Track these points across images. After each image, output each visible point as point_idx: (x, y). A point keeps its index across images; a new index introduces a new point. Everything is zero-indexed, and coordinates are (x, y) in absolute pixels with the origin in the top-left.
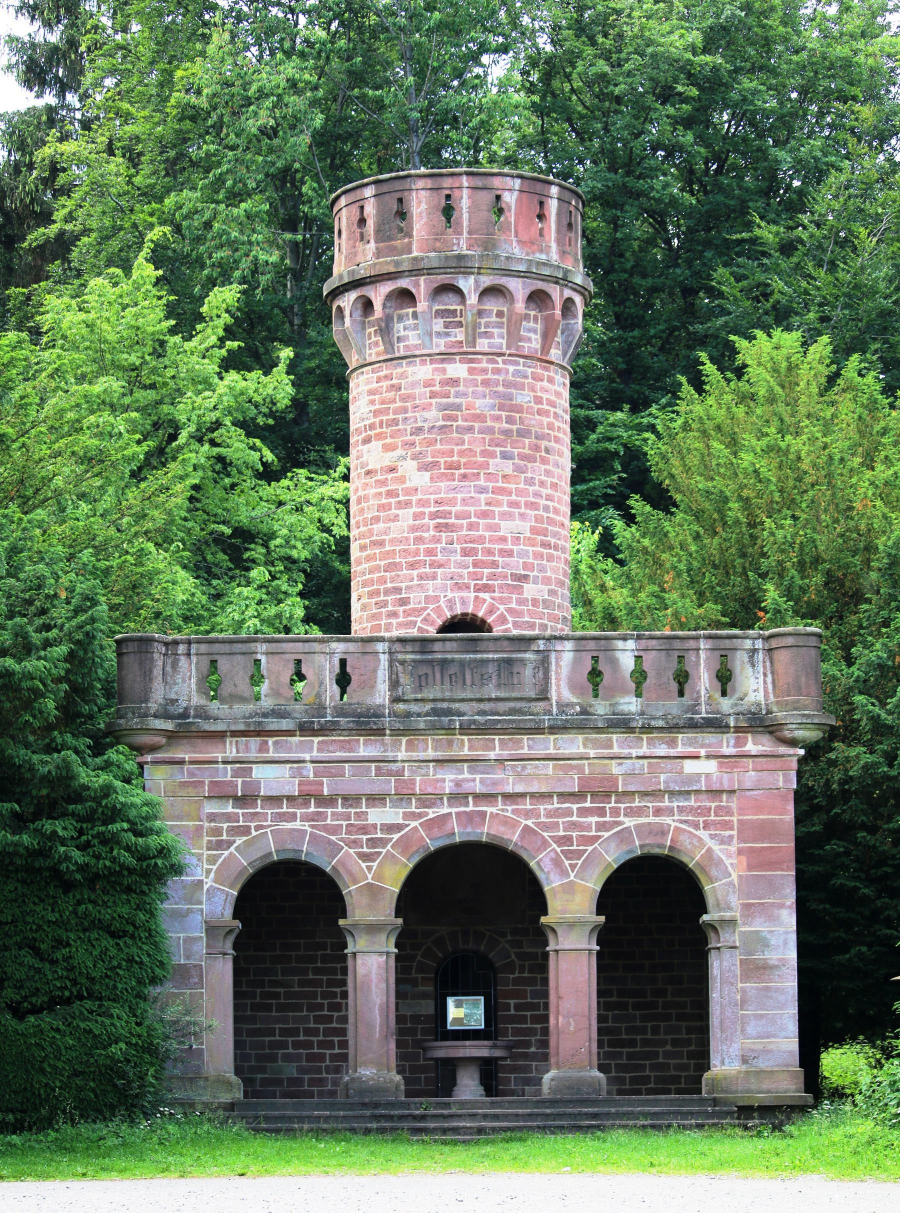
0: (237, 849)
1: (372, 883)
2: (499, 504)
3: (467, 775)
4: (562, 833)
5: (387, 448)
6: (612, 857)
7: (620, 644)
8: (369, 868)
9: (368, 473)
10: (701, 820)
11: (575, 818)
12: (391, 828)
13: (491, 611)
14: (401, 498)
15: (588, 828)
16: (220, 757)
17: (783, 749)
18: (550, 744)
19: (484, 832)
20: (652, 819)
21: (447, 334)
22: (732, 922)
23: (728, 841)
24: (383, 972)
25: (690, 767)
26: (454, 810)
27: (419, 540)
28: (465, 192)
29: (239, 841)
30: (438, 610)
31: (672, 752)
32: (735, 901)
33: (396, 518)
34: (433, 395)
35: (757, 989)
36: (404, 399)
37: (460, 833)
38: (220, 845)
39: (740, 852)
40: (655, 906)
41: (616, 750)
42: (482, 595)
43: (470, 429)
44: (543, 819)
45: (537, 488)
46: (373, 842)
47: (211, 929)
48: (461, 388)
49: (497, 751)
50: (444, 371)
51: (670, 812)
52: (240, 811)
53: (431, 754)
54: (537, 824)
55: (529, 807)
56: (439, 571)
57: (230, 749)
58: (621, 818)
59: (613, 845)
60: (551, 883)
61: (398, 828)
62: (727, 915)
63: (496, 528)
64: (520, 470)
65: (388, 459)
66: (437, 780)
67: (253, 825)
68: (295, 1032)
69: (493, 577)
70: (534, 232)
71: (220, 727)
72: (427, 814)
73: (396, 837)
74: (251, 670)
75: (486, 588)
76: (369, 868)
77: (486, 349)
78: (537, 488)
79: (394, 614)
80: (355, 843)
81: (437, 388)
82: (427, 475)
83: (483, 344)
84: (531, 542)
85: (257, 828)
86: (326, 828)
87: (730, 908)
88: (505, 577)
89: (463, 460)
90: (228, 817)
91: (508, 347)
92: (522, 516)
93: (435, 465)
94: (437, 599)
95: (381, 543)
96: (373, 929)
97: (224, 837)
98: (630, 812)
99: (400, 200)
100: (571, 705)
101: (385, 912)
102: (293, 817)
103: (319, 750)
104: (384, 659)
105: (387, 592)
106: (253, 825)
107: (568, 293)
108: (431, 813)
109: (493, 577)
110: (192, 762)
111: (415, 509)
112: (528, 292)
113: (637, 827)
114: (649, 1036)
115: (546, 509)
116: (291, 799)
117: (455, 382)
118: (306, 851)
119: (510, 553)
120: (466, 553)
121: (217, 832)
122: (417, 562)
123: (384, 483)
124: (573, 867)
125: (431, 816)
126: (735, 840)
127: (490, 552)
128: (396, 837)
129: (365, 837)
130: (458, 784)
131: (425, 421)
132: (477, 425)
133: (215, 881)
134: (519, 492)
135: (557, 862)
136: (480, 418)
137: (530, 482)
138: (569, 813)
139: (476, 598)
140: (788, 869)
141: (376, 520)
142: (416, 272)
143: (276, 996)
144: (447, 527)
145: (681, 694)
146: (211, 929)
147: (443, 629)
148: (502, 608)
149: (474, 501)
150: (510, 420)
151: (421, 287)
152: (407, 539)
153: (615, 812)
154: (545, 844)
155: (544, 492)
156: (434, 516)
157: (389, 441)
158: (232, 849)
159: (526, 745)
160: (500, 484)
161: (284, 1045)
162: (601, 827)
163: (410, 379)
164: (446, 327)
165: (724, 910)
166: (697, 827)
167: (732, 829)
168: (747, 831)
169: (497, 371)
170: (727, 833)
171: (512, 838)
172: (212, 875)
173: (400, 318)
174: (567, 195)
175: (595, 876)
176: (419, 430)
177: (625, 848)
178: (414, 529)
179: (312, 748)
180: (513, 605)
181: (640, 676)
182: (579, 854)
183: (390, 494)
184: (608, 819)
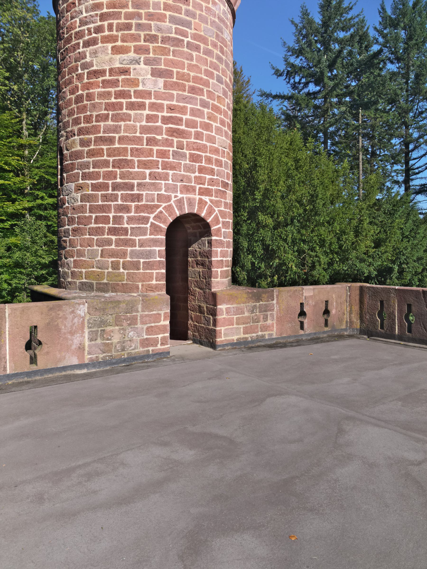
5: (116, 50)
27: (150, 141)
30: (169, 208)
33: (128, 118)
42: (203, 197)
56: (171, 172)
75: (207, 192)
79: (127, 209)
82: (161, 82)
94: (169, 198)
95: (111, 141)
111: (146, 112)
120: (195, 158)
122: (151, 162)
127: (209, 160)
131: (159, 29)
136: (204, 40)
139: (200, 199)
141: (106, 118)
144: (180, 133)
149: (200, 114)
156: (166, 120)
178: (144, 130)
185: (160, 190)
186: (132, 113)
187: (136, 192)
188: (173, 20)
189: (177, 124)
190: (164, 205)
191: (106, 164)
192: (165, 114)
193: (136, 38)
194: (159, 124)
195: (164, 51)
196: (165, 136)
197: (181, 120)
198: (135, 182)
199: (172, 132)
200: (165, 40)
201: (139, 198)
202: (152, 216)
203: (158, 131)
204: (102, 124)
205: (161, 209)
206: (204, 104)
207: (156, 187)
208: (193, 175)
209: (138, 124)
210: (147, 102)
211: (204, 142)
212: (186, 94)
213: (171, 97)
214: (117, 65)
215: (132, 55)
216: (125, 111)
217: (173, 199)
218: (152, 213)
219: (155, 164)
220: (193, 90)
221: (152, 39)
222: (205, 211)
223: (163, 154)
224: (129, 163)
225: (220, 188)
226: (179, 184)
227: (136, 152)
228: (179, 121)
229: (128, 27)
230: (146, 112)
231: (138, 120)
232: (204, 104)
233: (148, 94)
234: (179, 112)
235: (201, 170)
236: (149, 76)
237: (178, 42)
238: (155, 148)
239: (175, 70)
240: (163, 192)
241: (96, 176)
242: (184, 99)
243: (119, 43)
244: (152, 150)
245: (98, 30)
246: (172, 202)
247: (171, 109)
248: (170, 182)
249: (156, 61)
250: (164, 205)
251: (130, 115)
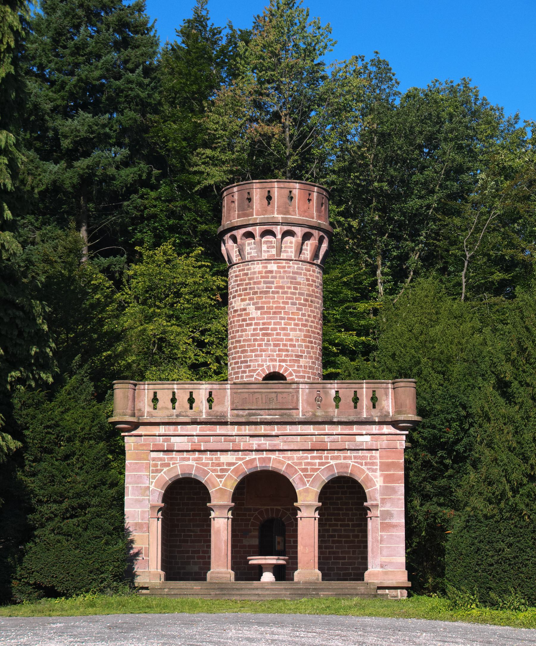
0: (165, 473)
1: (222, 489)
2: (290, 324)
3: (263, 442)
4: (303, 467)
5: (243, 300)
6: (325, 478)
7: (329, 386)
8: (221, 481)
10: (364, 461)
11: (309, 461)
12: (230, 464)
13: (286, 370)
14: (248, 322)
15: (314, 464)
16: (157, 433)
17: (398, 432)
18: (299, 429)
19: (271, 466)
20: (342, 461)
21: (268, 251)
22: (377, 506)
23: (375, 471)
24: (226, 526)
25: (359, 438)
26: (257, 457)
27: (255, 340)
28: (276, 189)
29: (165, 469)
30: (263, 370)
31: (351, 432)
32: (378, 497)
33: (245, 330)
34: (262, 277)
35: (387, 535)
36: (250, 279)
37: (259, 465)
38: (157, 471)
39: (381, 475)
40: (344, 499)
41: (327, 431)
42: (281, 364)
43: (278, 292)
44: (295, 461)
45: (307, 318)
46: (222, 470)
47: (153, 507)
48: (274, 274)
49: (276, 431)
50: (266, 267)
51: (350, 458)
52: (166, 456)
53: (247, 432)
54: (293, 463)
55: (289, 455)
56: (264, 353)
57: (162, 430)
58: (329, 461)
59: (325, 472)
60: (299, 489)
61: (233, 464)
62: (374, 503)
63: (288, 335)
64: (298, 309)
65: (242, 305)
66: (250, 444)
67: (171, 462)
68: (198, 552)
69: (287, 356)
70: (306, 207)
71: (158, 420)
72: (246, 458)
73: (232, 468)
74: (171, 396)
75: (284, 361)
76: (221, 481)
77: (285, 258)
78: (307, 318)
79: (244, 372)
80: (214, 471)
81: (264, 275)
82: (259, 312)
83: (284, 256)
84: (304, 341)
85: (173, 464)
86: (202, 464)
87: (376, 500)
88: (292, 356)
89: (274, 306)
90: (160, 459)
91: (295, 257)
92: (300, 330)
93: (262, 308)
94: (263, 365)
95: (239, 341)
96: (221, 507)
97: (159, 468)
98: (333, 458)
99: (249, 193)
100: (308, 412)
101: (227, 501)
102: (188, 459)
103: (200, 431)
104: (229, 391)
105: (242, 362)
106: (171, 462)
107: (321, 234)
108: (248, 458)
109: (287, 356)
110: (145, 436)
111: (253, 327)
112: (303, 233)
113: (336, 464)
114: (351, 555)
115: (311, 327)
116: (187, 451)
117: (271, 272)
118: (194, 473)
119: (294, 346)
120: (275, 345)
121: (156, 465)
124: (308, 481)
125: (248, 459)
126: (378, 471)
127: (285, 345)
128: (232, 468)
129: (219, 468)
130: (259, 445)
131: (258, 288)
132: (280, 290)
133: (155, 486)
134: (299, 319)
135: (301, 479)
136: (282, 287)
137: (304, 315)
138: (307, 458)
139: (280, 365)
143: (190, 536)
145: (355, 407)
146: (153, 507)
147: (265, 379)
148: (290, 369)
149: (280, 324)
150: (295, 288)
152: (250, 339)
153: (327, 458)
154: (296, 471)
155: (310, 319)
156: (261, 329)
157: (243, 297)
158: (162, 473)
159: (289, 429)
160: (290, 316)
161: (193, 558)
162: (321, 464)
163: (252, 270)
165: (373, 501)
166: (362, 465)
167: (377, 465)
168: (385, 466)
169: (289, 267)
170: (375, 467)
171: (282, 469)
172: (153, 484)
174: (322, 191)
175: (317, 486)
176: (255, 293)
177: (331, 473)
178: (253, 335)
179: (197, 430)
180: (296, 368)
181: (337, 399)
182: (311, 476)
183: (244, 320)
184: (323, 461)
186: (247, 328)
188: (265, 282)
193: (249, 294)
195: (261, 298)
197: (268, 328)
199: (264, 335)
200: (261, 293)
203: (257, 335)
206: (282, 318)
207: (257, 361)
210: (253, 322)
213: (264, 318)
214: (242, 307)
215: (248, 302)
219: (256, 350)
220: (275, 313)
223: (260, 345)
227: (249, 346)
228: (267, 329)
229: (246, 289)
230: (253, 327)
231: (250, 331)
232: (282, 318)
233: (253, 319)
235: (280, 350)
237: (267, 292)
238: (256, 343)
242: (270, 318)
247: (264, 324)
249: (257, 303)
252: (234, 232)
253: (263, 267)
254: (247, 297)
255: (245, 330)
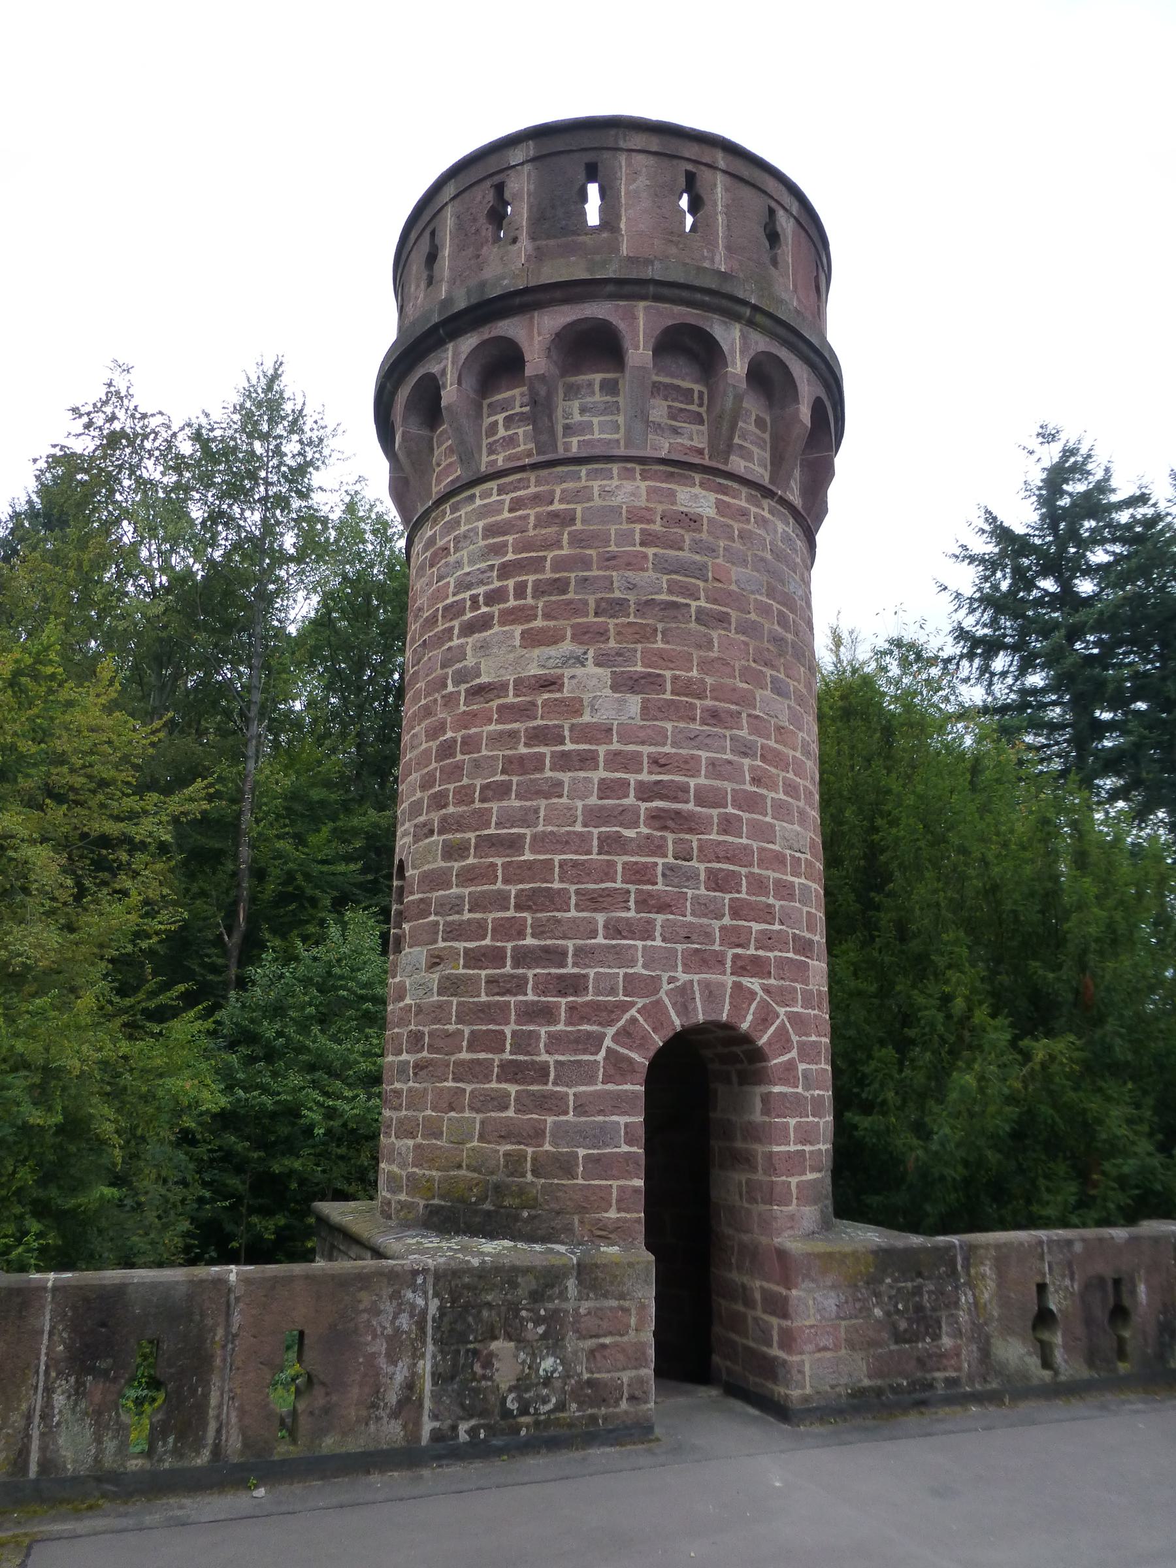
5: (532, 639)
9: (480, 691)
21: (675, 431)
27: (611, 844)
30: (655, 1012)
33: (555, 788)
36: (578, 540)
56: (660, 918)
75: (756, 967)
79: (546, 1014)
81: (657, 527)
82: (634, 703)
93: (652, 682)
94: (652, 985)
95: (513, 844)
117: (692, 521)
120: (718, 882)
122: (609, 893)
123: (524, 712)
127: (759, 885)
131: (631, 587)
139: (737, 986)
140: (638, 1212)
141: (502, 791)
142: (628, 288)
151: (640, 327)
152: (584, 838)
156: (647, 792)
163: (597, 502)
164: (672, 417)
173: (572, 391)
178: (595, 816)
183: (538, 736)
185: (632, 963)
186: (565, 777)
187: (570, 970)
189: (675, 799)
190: (641, 1002)
191: (501, 900)
192: (645, 777)
193: (576, 609)
194: (630, 800)
195: (645, 634)
196: (645, 830)
198: (570, 945)
201: (574, 985)
202: (611, 1031)
203: (627, 817)
204: (494, 806)
205: (633, 1012)
206: (745, 750)
207: (622, 957)
208: (716, 924)
209: (579, 804)
210: (602, 750)
211: (744, 841)
212: (696, 726)
214: (534, 670)
216: (548, 774)
217: (666, 987)
218: (610, 1023)
220: (714, 716)
221: (616, 607)
222: (750, 1017)
224: (555, 900)
225: (791, 955)
226: (679, 947)
228: (677, 792)
229: (560, 586)
232: (745, 750)
234: (679, 770)
236: (608, 692)
238: (620, 860)
239: (668, 674)
240: (639, 969)
241: (478, 930)
243: (539, 623)
244: (611, 864)
245: (494, 597)
246: (662, 994)
247: (657, 763)
248: (658, 942)
250: (641, 1002)
251: (560, 784)
252: (509, 328)
253: (651, 491)
254: (566, 625)
255: (555, 788)
